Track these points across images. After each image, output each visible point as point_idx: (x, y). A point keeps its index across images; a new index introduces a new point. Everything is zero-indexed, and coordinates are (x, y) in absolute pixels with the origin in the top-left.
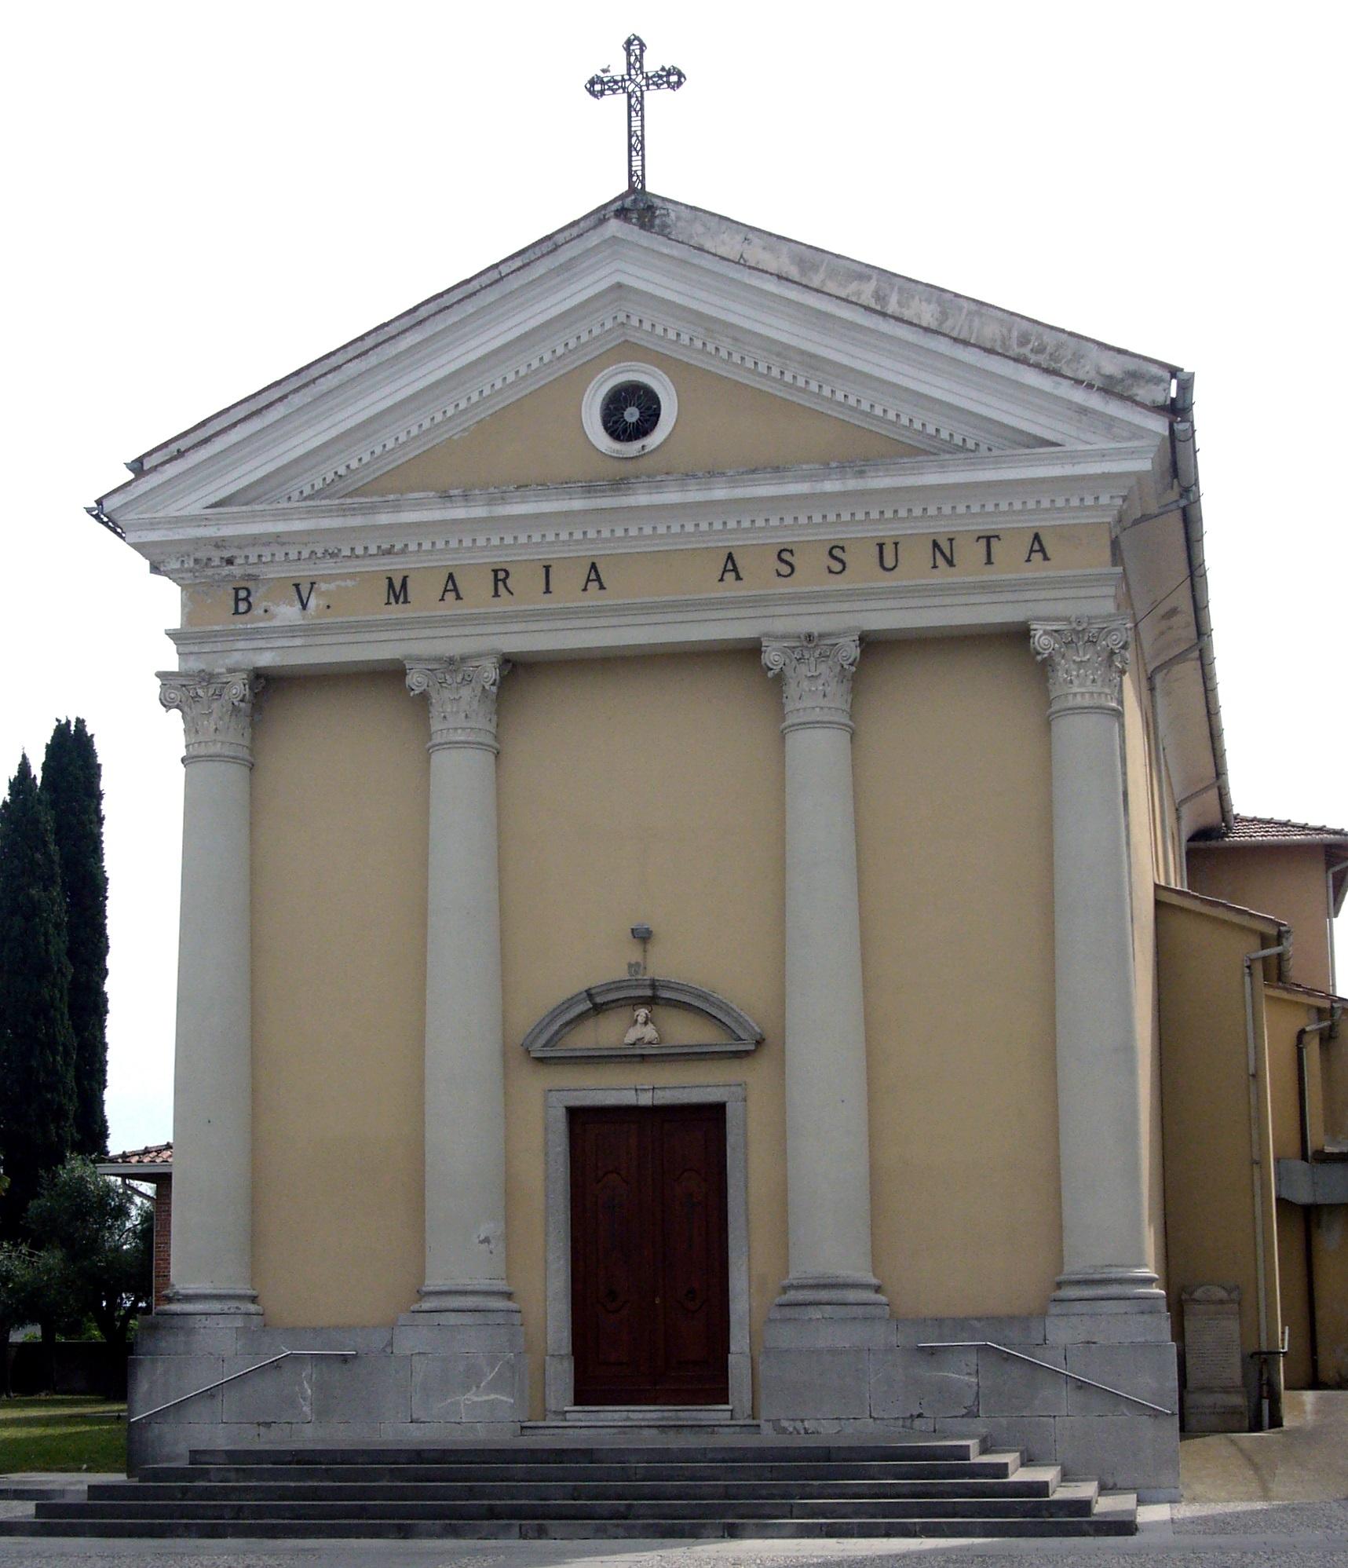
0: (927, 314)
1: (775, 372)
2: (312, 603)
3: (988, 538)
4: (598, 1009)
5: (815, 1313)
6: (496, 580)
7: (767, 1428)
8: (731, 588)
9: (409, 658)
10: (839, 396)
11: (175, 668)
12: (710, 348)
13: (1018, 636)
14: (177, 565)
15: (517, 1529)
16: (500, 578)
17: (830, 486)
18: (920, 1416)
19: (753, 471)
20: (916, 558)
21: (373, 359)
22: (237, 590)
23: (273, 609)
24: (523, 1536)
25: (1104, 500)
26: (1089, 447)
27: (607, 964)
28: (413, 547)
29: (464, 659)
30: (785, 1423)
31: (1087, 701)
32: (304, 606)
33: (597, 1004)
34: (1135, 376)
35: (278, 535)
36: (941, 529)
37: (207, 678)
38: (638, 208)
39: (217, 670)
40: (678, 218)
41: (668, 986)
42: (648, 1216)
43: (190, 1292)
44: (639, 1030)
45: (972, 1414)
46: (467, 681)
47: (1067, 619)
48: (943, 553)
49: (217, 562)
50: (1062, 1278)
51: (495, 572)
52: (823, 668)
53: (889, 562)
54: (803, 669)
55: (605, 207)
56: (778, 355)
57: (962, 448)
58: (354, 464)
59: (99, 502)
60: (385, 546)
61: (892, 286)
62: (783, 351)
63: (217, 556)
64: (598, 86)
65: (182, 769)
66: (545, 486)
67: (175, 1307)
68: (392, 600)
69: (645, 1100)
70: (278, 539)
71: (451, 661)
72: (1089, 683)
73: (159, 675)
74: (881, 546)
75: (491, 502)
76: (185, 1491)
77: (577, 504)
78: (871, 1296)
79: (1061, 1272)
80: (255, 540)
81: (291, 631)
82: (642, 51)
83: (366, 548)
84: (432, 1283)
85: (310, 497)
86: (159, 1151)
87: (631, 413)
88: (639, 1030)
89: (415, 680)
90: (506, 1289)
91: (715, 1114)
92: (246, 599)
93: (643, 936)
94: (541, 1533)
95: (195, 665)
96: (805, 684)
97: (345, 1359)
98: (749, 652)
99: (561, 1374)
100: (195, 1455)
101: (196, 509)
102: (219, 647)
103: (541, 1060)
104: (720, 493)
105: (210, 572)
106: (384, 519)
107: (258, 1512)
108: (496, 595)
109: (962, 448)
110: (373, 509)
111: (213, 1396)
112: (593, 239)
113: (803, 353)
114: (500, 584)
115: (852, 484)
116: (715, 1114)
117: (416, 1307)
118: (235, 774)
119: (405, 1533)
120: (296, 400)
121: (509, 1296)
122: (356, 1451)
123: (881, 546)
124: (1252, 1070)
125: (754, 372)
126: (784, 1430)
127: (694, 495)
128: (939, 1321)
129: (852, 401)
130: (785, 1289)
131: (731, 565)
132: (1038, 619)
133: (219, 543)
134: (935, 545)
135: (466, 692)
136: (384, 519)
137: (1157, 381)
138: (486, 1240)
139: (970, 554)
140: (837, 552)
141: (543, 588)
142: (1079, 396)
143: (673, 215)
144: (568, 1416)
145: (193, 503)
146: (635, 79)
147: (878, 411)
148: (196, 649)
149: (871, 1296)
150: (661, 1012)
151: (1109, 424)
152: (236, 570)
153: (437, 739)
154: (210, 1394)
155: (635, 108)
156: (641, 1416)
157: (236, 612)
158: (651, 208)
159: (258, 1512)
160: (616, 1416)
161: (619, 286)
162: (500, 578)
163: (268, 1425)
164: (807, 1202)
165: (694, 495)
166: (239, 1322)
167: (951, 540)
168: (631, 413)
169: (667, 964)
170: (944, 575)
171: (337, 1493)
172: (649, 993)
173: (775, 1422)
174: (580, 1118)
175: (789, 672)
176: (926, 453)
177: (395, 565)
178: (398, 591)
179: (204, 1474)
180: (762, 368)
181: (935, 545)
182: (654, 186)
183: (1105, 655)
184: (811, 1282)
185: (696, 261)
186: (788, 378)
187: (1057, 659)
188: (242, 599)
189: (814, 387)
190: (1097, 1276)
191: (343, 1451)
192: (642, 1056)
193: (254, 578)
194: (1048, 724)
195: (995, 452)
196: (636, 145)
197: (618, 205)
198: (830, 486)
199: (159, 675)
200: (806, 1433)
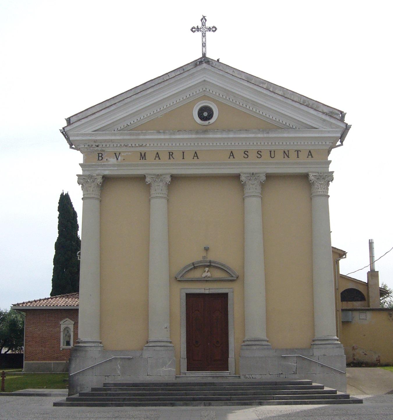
0: (280, 93)
1: (244, 106)
2: (120, 158)
3: (298, 151)
4: (195, 268)
5: (255, 347)
6: (170, 155)
7: (242, 377)
8: (232, 160)
9: (147, 174)
10: (261, 113)
11: (82, 174)
12: (228, 98)
13: (306, 176)
14: (83, 146)
15: (203, 404)
16: (171, 154)
17: (259, 135)
18: (282, 374)
19: (240, 130)
21: (139, 95)
22: (99, 154)
23: (109, 159)
24: (205, 405)
25: (328, 143)
26: (325, 130)
27: (197, 256)
28: (148, 145)
29: (161, 175)
30: (247, 376)
31: (322, 193)
32: (117, 159)
33: (195, 267)
34: (331, 112)
35: (112, 140)
36: (286, 148)
37: (90, 177)
38: (204, 60)
39: (93, 175)
40: (216, 65)
41: (215, 262)
42: (207, 321)
43: (86, 340)
44: (207, 273)
45: (295, 373)
46: (161, 181)
47: (318, 173)
48: (286, 154)
49: (94, 146)
50: (314, 339)
51: (170, 153)
52: (255, 182)
53: (273, 156)
54: (250, 182)
55: (196, 60)
56: (246, 101)
57: (292, 128)
58: (132, 122)
59: (64, 128)
60: (140, 144)
61: (271, 86)
62: (247, 100)
63: (94, 144)
64: (194, 30)
65: (82, 201)
66: (185, 131)
67: (80, 345)
68: (141, 159)
69: (207, 292)
70: (111, 141)
71: (158, 175)
72: (323, 189)
73: (77, 175)
74: (271, 151)
75: (171, 134)
76: (106, 395)
77: (194, 136)
78: (266, 343)
79: (314, 338)
80: (105, 141)
81: (114, 165)
82: (206, 21)
83: (135, 145)
84: (151, 339)
85: (120, 130)
87: (206, 114)
88: (207, 273)
89: (148, 180)
90: (171, 341)
91: (225, 296)
92: (101, 156)
93: (207, 249)
94: (210, 405)
95: (87, 173)
96: (251, 186)
97: (129, 359)
98: (237, 177)
99: (184, 363)
100: (105, 385)
101: (90, 132)
102: (94, 169)
103: (179, 281)
104: (231, 135)
105: (92, 149)
106: (141, 137)
107: (130, 400)
108: (170, 159)
109: (292, 128)
110: (139, 134)
111: (93, 368)
112: (199, 68)
113: (252, 101)
114: (171, 156)
115: (265, 135)
116: (225, 296)
117: (146, 345)
118: (97, 202)
119: (173, 405)
120: (119, 105)
121: (171, 342)
122: (150, 383)
123: (271, 151)
124: (337, 288)
126: (247, 378)
127: (224, 136)
128: (287, 349)
129: (264, 114)
130: (244, 342)
132: (311, 172)
133: (95, 141)
134: (284, 152)
135: (161, 184)
136: (141, 137)
137: (338, 114)
138: (166, 328)
140: (259, 152)
141: (182, 158)
142: (324, 117)
143: (214, 64)
144: (186, 374)
145: (89, 130)
146: (203, 28)
147: (271, 117)
149: (266, 343)
150: (212, 269)
151: (331, 124)
152: (99, 149)
153: (152, 196)
154: (92, 368)
155: (204, 36)
156: (211, 374)
158: (208, 62)
159: (130, 400)
160: (200, 374)
161: (205, 81)
162: (171, 154)
163: (108, 376)
164: (250, 318)
165: (224, 136)
166: (99, 349)
167: (288, 151)
168: (206, 114)
169: (212, 256)
170: (286, 160)
173: (245, 376)
174: (189, 296)
175: (247, 183)
177: (142, 149)
179: (110, 390)
181: (284, 152)
182: (207, 56)
183: (327, 182)
184: (253, 339)
185: (226, 76)
186: (248, 107)
187: (315, 182)
188: (100, 156)
189: (254, 110)
190: (326, 338)
192: (207, 281)
193: (103, 151)
196: (204, 45)
197: (200, 60)
198: (259, 135)
199: (77, 175)
200: (253, 378)
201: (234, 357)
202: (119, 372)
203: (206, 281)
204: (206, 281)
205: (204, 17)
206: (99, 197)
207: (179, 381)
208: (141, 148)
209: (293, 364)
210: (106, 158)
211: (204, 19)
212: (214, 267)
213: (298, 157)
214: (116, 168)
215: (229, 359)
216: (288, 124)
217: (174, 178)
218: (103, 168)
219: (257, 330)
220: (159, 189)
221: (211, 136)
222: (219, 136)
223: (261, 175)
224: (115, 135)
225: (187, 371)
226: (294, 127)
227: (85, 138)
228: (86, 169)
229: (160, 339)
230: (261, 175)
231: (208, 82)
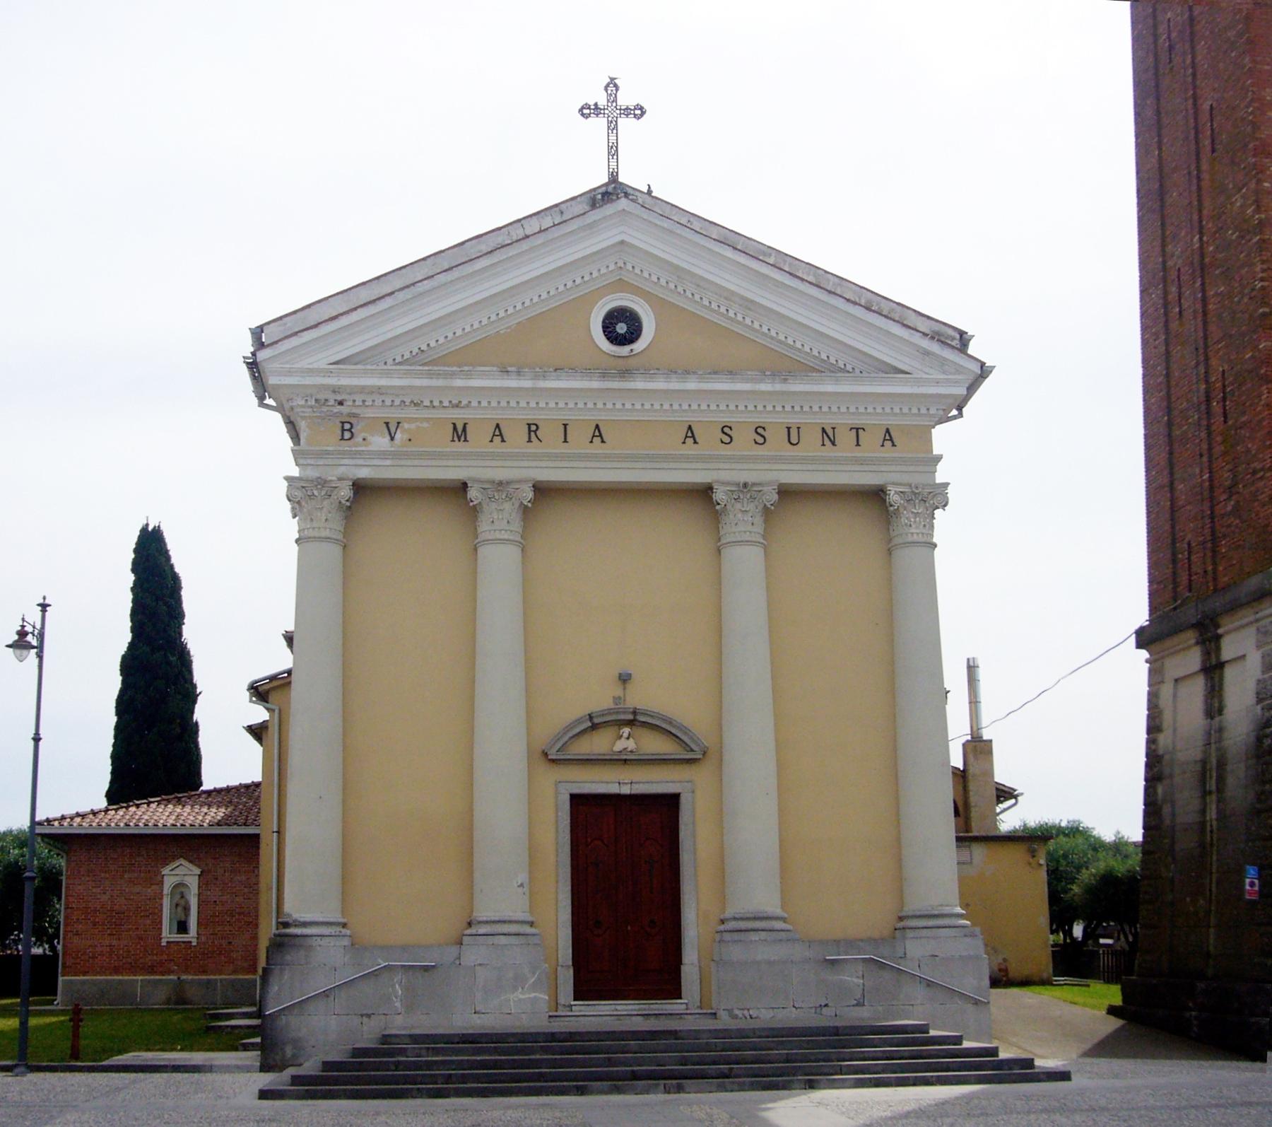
1: (723, 310)
2: (398, 436)
4: (594, 727)
5: (754, 937)
6: (530, 431)
7: (723, 1015)
8: (690, 449)
11: (297, 475)
12: (680, 289)
14: (303, 402)
16: (533, 430)
17: (765, 387)
18: (826, 1005)
19: (715, 373)
20: (811, 439)
21: (455, 274)
22: (343, 423)
23: (369, 438)
24: (667, 1091)
25: (933, 411)
26: (925, 376)
27: (600, 699)
28: (474, 404)
29: (508, 483)
32: (392, 439)
33: (594, 724)
36: (828, 421)
37: (321, 483)
42: (626, 870)
43: (308, 920)
44: (625, 743)
45: (860, 1004)
49: (332, 402)
50: (904, 914)
53: (794, 440)
54: (738, 506)
55: (595, 189)
58: (433, 344)
61: (785, 261)
62: (729, 296)
63: (332, 398)
64: (589, 111)
65: (296, 548)
69: (626, 790)
70: (379, 390)
71: (500, 483)
73: (287, 478)
74: (789, 428)
77: (595, 384)
79: (901, 910)
80: (362, 390)
81: (383, 455)
86: (72, 818)
87: (622, 327)
88: (625, 743)
89: (473, 493)
91: (672, 801)
92: (350, 430)
93: (624, 679)
94: (680, 1089)
95: (312, 473)
96: (740, 515)
97: (426, 969)
98: (704, 493)
100: (386, 1039)
101: (322, 365)
102: (330, 462)
103: (553, 761)
104: (692, 385)
105: (325, 409)
106: (459, 383)
107: (464, 1079)
108: (530, 441)
109: (844, 370)
110: (452, 375)
112: (609, 209)
115: (779, 387)
116: (672, 801)
118: (336, 550)
119: (581, 1091)
120: (401, 296)
121: (532, 924)
123: (789, 428)
125: (709, 308)
126: (736, 1017)
127: (675, 385)
128: (837, 942)
129: (773, 333)
130: (722, 922)
131: (690, 433)
132: (893, 484)
133: (335, 390)
134: (824, 430)
135: (507, 506)
136: (459, 383)
137: (953, 339)
138: (522, 885)
139: (845, 438)
142: (925, 343)
145: (321, 359)
146: (611, 110)
148: (311, 462)
150: (639, 732)
154: (325, 994)
155: (613, 127)
157: (342, 439)
159: (464, 1079)
161: (622, 242)
162: (533, 430)
163: (369, 1016)
164: (737, 862)
165: (675, 385)
166: (346, 942)
168: (622, 327)
169: (638, 698)
171: (495, 1064)
172: (631, 717)
173: (730, 1011)
174: (578, 801)
176: (814, 370)
177: (459, 415)
178: (460, 433)
180: (714, 306)
181: (824, 430)
182: (621, 179)
186: (731, 314)
187: (901, 510)
188: (347, 429)
189: (748, 321)
191: (531, 1034)
192: (625, 760)
193: (355, 416)
194: (890, 552)
195: (865, 374)
196: (613, 151)
197: (604, 189)
198: (765, 387)
199: (287, 478)
201: (696, 961)
202: (398, 1004)
203: (623, 761)
204: (623, 761)
205: (612, 79)
206: (340, 537)
207: (558, 1026)
208: (456, 411)
209: (856, 980)
210: (363, 435)
211: (612, 85)
212: (644, 724)
213: (858, 445)
215: (683, 968)
216: (832, 360)
217: (543, 491)
219: (758, 892)
220: (500, 521)
221: (639, 384)
222: (659, 384)
223: (765, 489)
224: (388, 374)
225: (575, 999)
226: (849, 368)
227: (308, 381)
228: (309, 461)
229: (508, 914)
230: (765, 489)
231: (632, 246)
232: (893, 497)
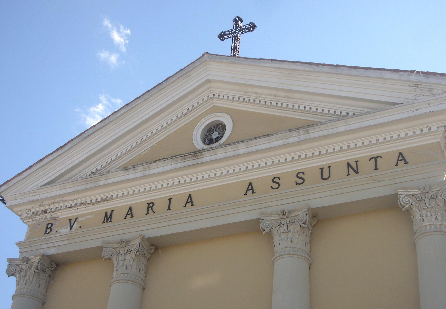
3: (375, 158)
32: (71, 227)
36: (350, 157)
39: (31, 257)
53: (325, 176)
60: (104, 197)
68: (105, 221)
72: (433, 219)
74: (322, 169)
92: (50, 228)
108: (148, 213)
114: (150, 208)
167: (356, 162)
188: (49, 228)
193: (55, 219)
210: (56, 230)
214: (65, 242)
218: (48, 245)
223: (300, 213)
232: (405, 199)
